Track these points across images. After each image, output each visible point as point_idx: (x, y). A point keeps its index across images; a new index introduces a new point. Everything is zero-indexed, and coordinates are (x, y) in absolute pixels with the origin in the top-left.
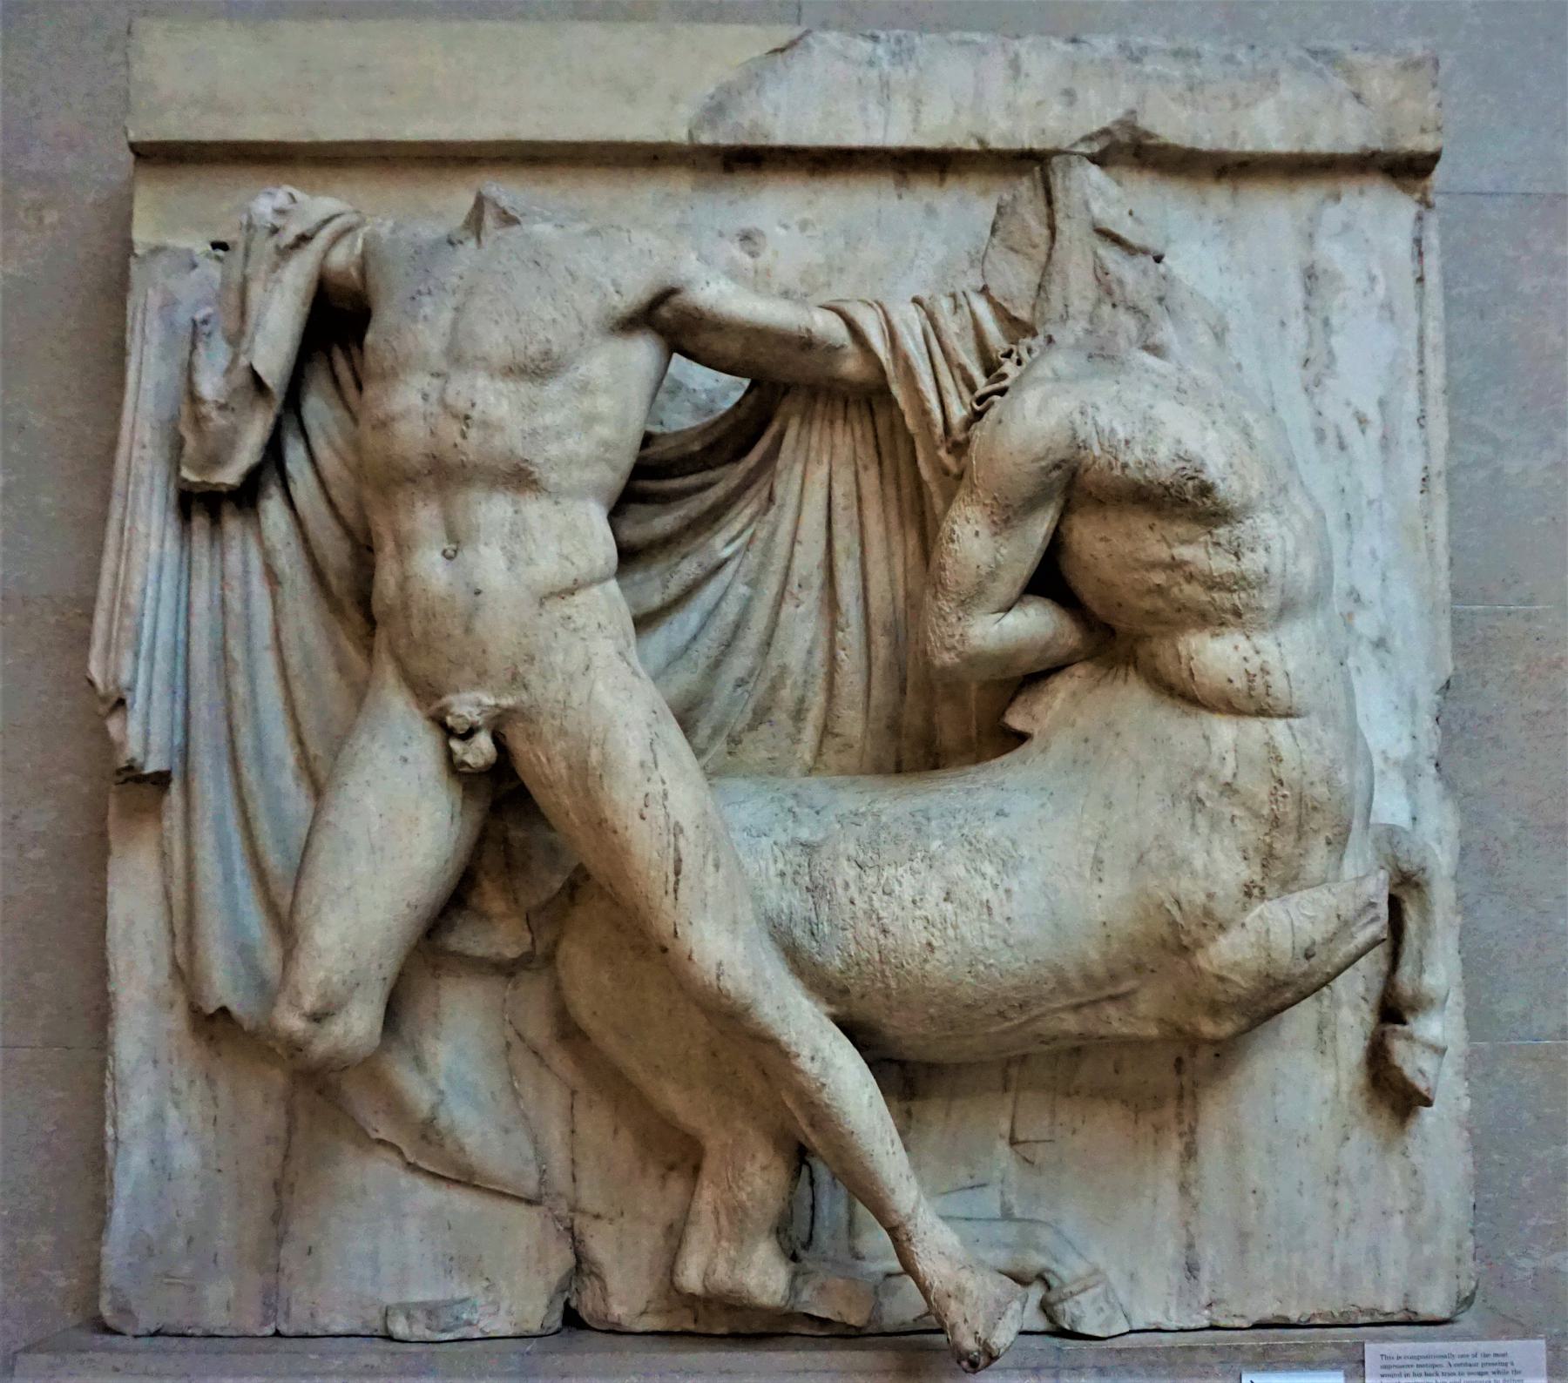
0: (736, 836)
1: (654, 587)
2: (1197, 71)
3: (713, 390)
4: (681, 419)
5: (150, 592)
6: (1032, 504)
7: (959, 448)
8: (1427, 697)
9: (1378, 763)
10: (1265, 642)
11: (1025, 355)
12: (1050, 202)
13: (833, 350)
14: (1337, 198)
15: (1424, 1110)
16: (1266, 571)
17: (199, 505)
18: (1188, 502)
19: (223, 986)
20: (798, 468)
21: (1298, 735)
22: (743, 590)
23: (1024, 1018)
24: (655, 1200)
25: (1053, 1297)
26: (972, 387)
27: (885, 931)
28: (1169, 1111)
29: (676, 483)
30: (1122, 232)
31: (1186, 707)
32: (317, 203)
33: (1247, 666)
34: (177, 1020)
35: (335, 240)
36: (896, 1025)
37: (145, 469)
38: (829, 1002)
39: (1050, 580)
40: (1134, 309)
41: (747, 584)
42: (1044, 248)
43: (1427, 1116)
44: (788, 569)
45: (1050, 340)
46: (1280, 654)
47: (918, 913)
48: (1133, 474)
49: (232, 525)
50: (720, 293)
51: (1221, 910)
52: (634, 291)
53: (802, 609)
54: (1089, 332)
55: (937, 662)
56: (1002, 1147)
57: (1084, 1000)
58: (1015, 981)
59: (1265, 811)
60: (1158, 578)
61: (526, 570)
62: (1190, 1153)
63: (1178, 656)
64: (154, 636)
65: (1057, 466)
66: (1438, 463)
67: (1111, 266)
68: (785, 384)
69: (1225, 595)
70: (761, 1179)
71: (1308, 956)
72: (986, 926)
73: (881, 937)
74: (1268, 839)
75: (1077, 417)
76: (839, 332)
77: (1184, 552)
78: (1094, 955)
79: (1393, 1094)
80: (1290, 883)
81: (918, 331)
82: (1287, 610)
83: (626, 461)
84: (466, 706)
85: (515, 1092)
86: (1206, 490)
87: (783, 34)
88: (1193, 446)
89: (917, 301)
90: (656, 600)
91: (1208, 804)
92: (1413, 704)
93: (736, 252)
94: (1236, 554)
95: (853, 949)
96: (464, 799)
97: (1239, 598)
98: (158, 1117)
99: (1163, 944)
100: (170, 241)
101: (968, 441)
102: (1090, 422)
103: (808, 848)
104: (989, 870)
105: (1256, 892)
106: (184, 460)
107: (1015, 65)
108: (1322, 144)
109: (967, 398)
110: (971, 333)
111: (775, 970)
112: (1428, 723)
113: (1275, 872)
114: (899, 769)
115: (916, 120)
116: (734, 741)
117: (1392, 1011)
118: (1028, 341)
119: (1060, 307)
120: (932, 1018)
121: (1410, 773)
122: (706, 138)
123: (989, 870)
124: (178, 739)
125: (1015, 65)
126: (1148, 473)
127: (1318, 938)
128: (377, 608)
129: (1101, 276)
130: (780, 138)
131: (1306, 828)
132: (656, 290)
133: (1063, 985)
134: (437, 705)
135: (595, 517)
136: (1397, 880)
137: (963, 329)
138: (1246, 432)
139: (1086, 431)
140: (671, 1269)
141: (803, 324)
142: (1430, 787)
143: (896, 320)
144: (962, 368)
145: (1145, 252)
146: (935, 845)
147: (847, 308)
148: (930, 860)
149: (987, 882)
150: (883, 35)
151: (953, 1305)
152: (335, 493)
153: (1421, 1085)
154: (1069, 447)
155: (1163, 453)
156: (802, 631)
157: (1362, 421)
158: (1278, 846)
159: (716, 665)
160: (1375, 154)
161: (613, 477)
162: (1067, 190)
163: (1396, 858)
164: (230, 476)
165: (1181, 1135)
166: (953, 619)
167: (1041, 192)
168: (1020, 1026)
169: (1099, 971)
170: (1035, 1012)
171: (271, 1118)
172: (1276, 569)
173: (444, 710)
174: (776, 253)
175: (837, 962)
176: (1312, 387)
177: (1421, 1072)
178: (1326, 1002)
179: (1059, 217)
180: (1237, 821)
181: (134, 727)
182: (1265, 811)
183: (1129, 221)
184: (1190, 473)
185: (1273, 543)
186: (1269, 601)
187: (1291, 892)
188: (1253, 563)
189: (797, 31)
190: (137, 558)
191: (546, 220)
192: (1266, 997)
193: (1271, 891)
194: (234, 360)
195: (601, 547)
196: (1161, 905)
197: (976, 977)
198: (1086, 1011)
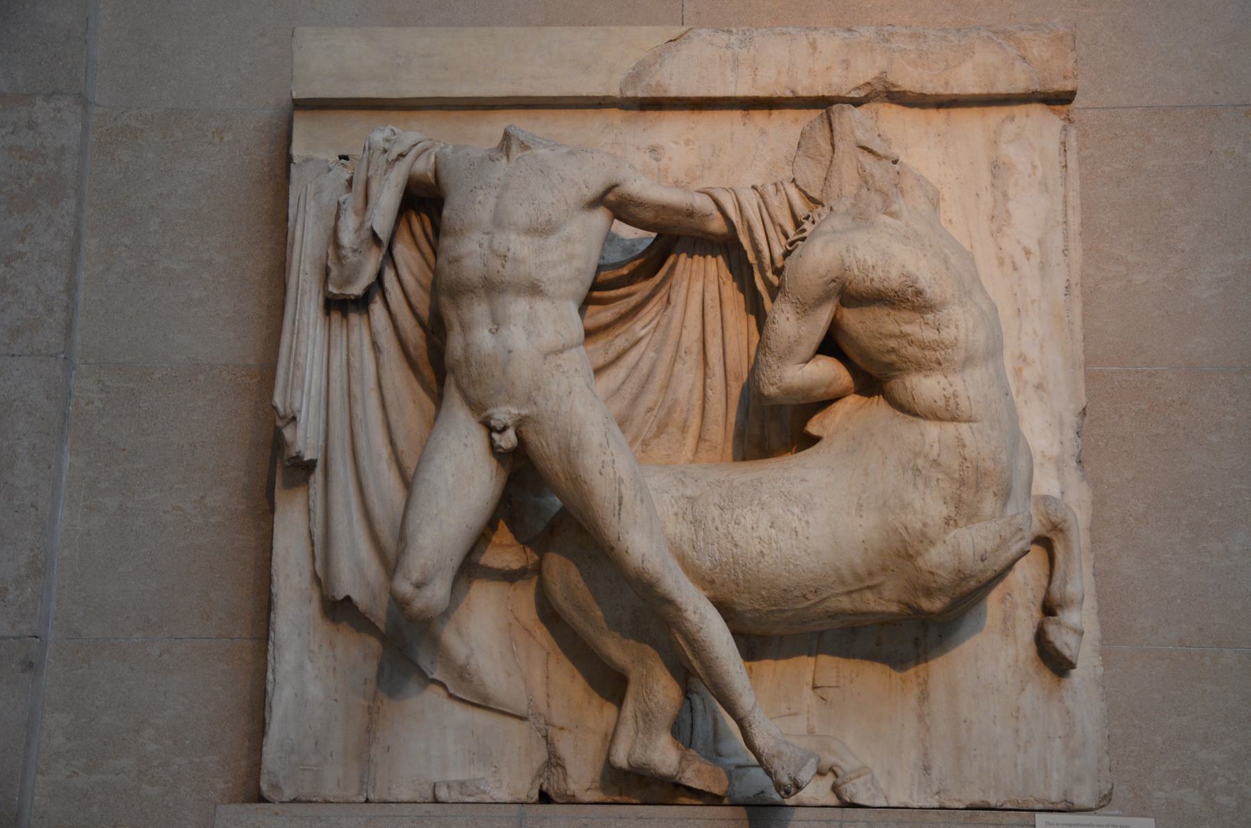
0: (652, 493)
1: (602, 350)
2: (925, 47)
4: (616, 256)
6: (820, 301)
7: (778, 272)
8: (1071, 419)
9: (1037, 459)
10: (956, 380)
11: (816, 219)
12: (832, 131)
15: (1073, 671)
17: (338, 306)
19: (347, 584)
20: (685, 284)
22: (652, 354)
23: (817, 600)
24: (600, 715)
25: (839, 781)
26: (787, 237)
27: (736, 545)
28: (911, 671)
29: (613, 293)
30: (875, 149)
31: (911, 418)
32: (410, 133)
34: (314, 609)
36: (744, 602)
37: (307, 287)
38: (704, 589)
39: (831, 345)
40: (880, 191)
42: (828, 157)
43: (1076, 675)
44: (679, 343)
46: (966, 387)
48: (876, 284)
49: (354, 318)
51: (931, 533)
52: (595, 187)
54: (854, 205)
55: (766, 393)
56: (807, 690)
57: (852, 588)
58: (811, 575)
59: (956, 476)
60: (892, 343)
61: (533, 342)
62: (924, 697)
63: (906, 388)
64: (310, 382)
66: (1076, 278)
67: (867, 167)
70: (663, 691)
72: (794, 542)
73: (734, 550)
75: (844, 253)
76: (710, 206)
77: (908, 329)
78: (858, 561)
79: (1055, 662)
80: (972, 517)
81: (755, 204)
82: (969, 361)
83: (588, 281)
84: (503, 414)
86: (919, 293)
87: (677, 31)
88: (911, 268)
89: (753, 187)
90: (601, 361)
92: (1061, 423)
95: (717, 555)
97: (939, 355)
98: (300, 667)
99: (898, 554)
100: (315, 155)
101: (783, 267)
104: (797, 511)
106: (330, 281)
108: (1001, 88)
109: (784, 241)
110: (787, 205)
111: (673, 563)
112: (1070, 434)
113: (962, 510)
114: (744, 459)
115: (754, 80)
116: (645, 444)
118: (820, 209)
120: (762, 597)
121: (1059, 464)
122: (630, 93)
123: (797, 511)
124: (321, 443)
125: (813, 46)
127: (988, 549)
128: (449, 361)
129: (861, 171)
130: (673, 92)
134: (484, 414)
135: (573, 308)
137: (781, 203)
138: (945, 261)
139: (850, 261)
140: (609, 754)
142: (1073, 475)
143: (742, 199)
144: (781, 226)
145: (886, 158)
146: (765, 497)
147: (717, 194)
150: (735, 31)
151: (776, 761)
152: (414, 300)
153: (1066, 652)
155: (894, 273)
156: (688, 378)
157: (1028, 253)
158: (964, 496)
159: (636, 399)
161: (582, 289)
162: (841, 124)
164: (356, 289)
165: (919, 684)
166: (775, 367)
167: (827, 126)
168: (815, 604)
170: (825, 595)
171: (370, 670)
172: (962, 337)
174: (670, 159)
175: (708, 564)
176: (997, 233)
179: (836, 139)
181: (300, 432)
182: (956, 476)
183: (878, 139)
185: (959, 324)
186: (959, 356)
188: (948, 334)
189: (684, 29)
190: (303, 336)
191: (545, 147)
192: (959, 585)
193: (961, 522)
194: (362, 224)
195: (576, 326)
196: (896, 531)
198: (854, 595)
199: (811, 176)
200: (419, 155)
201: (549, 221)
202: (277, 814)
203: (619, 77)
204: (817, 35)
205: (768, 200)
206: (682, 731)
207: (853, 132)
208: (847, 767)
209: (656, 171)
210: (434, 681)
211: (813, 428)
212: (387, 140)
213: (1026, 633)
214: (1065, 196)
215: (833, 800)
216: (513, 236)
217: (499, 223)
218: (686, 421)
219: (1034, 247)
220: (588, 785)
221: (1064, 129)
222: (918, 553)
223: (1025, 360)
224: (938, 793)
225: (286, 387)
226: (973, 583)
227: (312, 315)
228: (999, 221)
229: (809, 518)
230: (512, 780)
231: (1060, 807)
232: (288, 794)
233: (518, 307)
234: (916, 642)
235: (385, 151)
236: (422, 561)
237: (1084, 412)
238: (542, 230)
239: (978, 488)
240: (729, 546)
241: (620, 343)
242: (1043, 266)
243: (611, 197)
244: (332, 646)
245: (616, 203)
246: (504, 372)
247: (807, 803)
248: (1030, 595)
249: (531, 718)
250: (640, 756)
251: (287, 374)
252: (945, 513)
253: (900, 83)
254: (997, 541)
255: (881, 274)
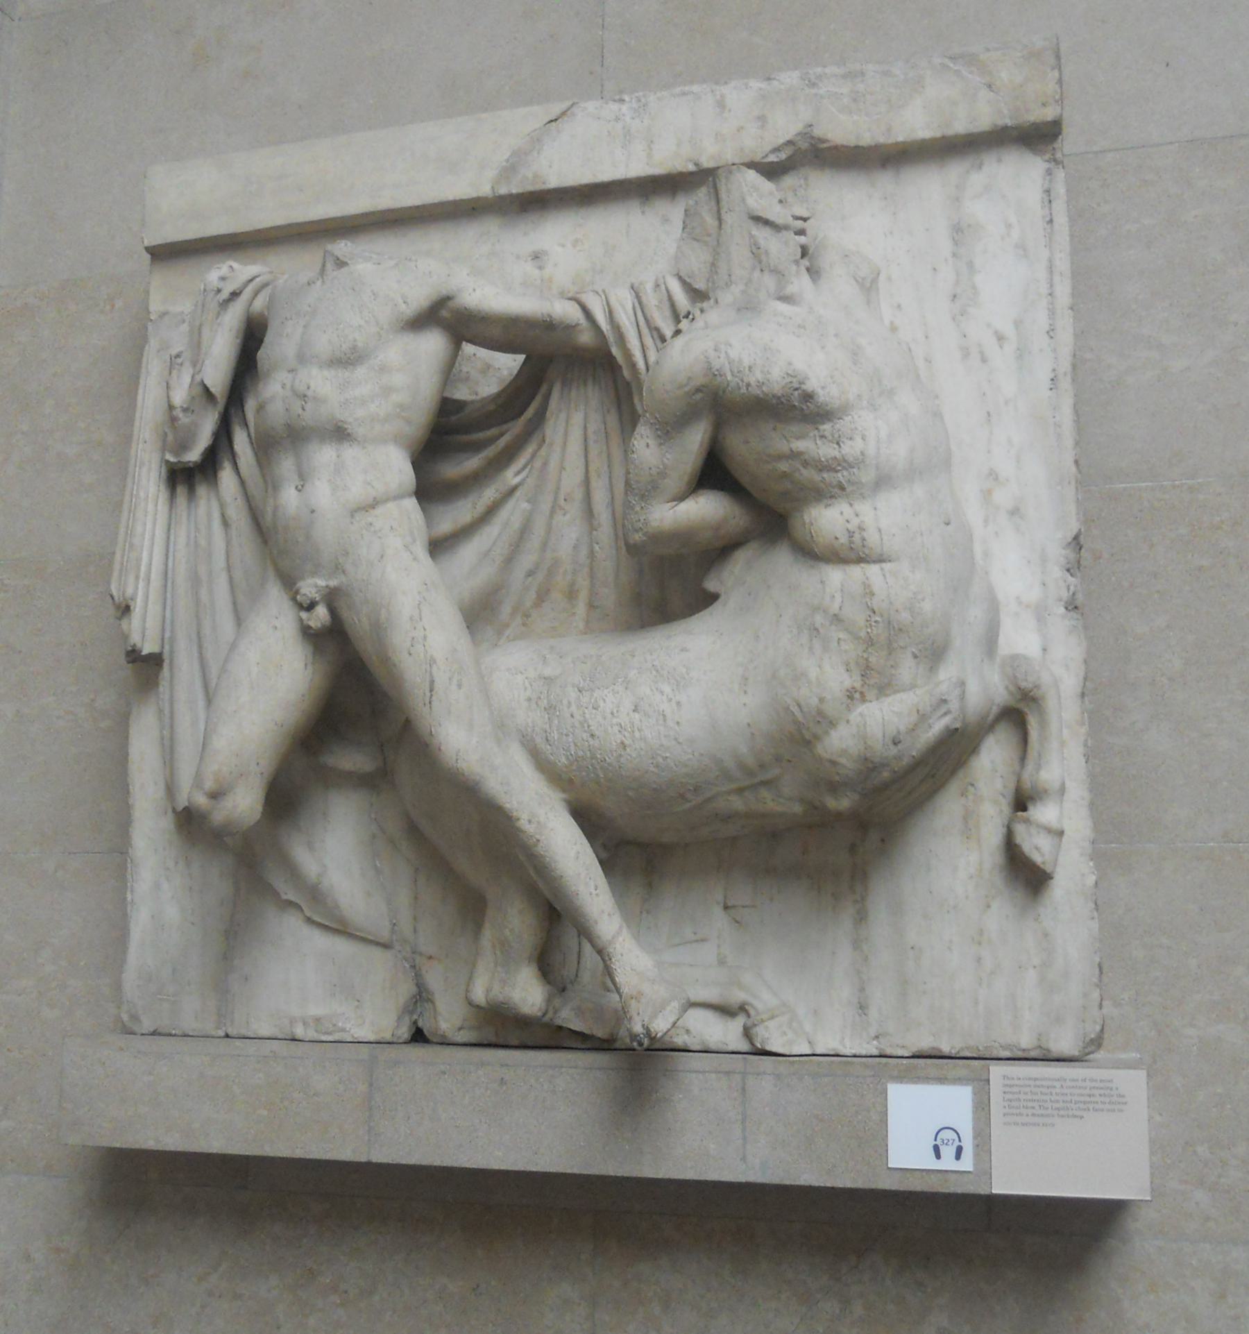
3: (496, 369)
5: (147, 536)
8: (1058, 553)
10: (864, 508)
12: (718, 201)
13: (571, 328)
14: (980, 167)
16: (862, 453)
18: (796, 408)
21: (888, 575)
27: (592, 735)
30: (771, 217)
33: (850, 526)
35: (256, 293)
38: (564, 791)
39: (714, 473)
40: (775, 271)
41: (528, 501)
43: (1062, 888)
44: (558, 488)
45: (717, 302)
47: (615, 721)
50: (491, 294)
51: (829, 709)
53: (568, 516)
56: (718, 911)
59: (863, 634)
60: (783, 466)
62: (861, 917)
65: (698, 390)
66: (1065, 365)
67: (762, 243)
68: (561, 360)
69: (832, 474)
71: (895, 744)
72: (662, 728)
74: (865, 655)
75: (712, 354)
77: (799, 445)
78: (744, 749)
80: (884, 689)
81: (629, 307)
82: (883, 482)
85: (376, 868)
86: (808, 397)
87: (556, 109)
88: (800, 365)
91: (821, 631)
92: (1044, 560)
93: (530, 268)
94: (838, 443)
96: (314, 654)
97: (841, 476)
102: (723, 355)
103: (549, 680)
104: (667, 689)
105: (857, 695)
107: (721, 105)
108: (960, 126)
110: (666, 306)
112: (1057, 572)
113: (873, 680)
117: (1021, 802)
119: (726, 277)
121: (1040, 613)
122: (503, 190)
123: (667, 689)
126: (764, 389)
127: (902, 728)
129: (756, 252)
130: (554, 181)
131: (895, 645)
132: (434, 297)
133: (726, 775)
136: (1019, 697)
138: (855, 354)
139: (718, 362)
141: (544, 311)
142: (1060, 622)
144: (657, 330)
146: (632, 674)
148: (627, 684)
149: (664, 698)
150: (627, 98)
153: (1037, 858)
154: (706, 375)
158: (873, 659)
160: (1005, 129)
162: (728, 191)
163: (1015, 677)
164: (194, 455)
166: (638, 508)
169: (750, 761)
170: (708, 794)
172: (871, 451)
173: (297, 592)
175: (564, 760)
177: (1037, 848)
178: (971, 797)
179: (723, 211)
180: (842, 643)
182: (863, 634)
184: (796, 385)
186: (867, 476)
187: (887, 696)
188: (850, 449)
193: (871, 694)
196: (788, 708)
197: (657, 766)
198: (746, 794)
199: (696, 262)
200: (256, 293)
201: (354, 348)
202: (122, 1049)
203: (490, 174)
204: (725, 90)
205: (644, 299)
206: (546, 963)
207: (744, 200)
208: (759, 1006)
209: (539, 282)
210: (291, 904)
211: (711, 585)
212: (223, 279)
213: (992, 836)
214: (1050, 261)
215: (744, 1046)
216: (315, 371)
217: (303, 358)
218: (573, 584)
219: (1008, 330)
220: (458, 1023)
221: (1049, 172)
222: (817, 737)
223: (996, 479)
224: (877, 1037)
225: (121, 570)
226: (886, 774)
227: (152, 489)
228: (962, 300)
229: (682, 697)
230: (373, 1015)
231: (1033, 1054)
232: (147, 1025)
233: (324, 455)
234: (853, 849)
235: (219, 291)
236: (216, 767)
237: (1076, 542)
238: (347, 360)
239: (890, 649)
240: (585, 736)
241: (489, 494)
242: (1021, 354)
243: (444, 313)
244: (188, 863)
245: (452, 321)
246: (308, 537)
247: (714, 1047)
248: (999, 784)
249: (397, 947)
250: (498, 993)
251: (123, 557)
252: (848, 683)
253: (829, 136)
254: (914, 718)
255: (759, 376)
